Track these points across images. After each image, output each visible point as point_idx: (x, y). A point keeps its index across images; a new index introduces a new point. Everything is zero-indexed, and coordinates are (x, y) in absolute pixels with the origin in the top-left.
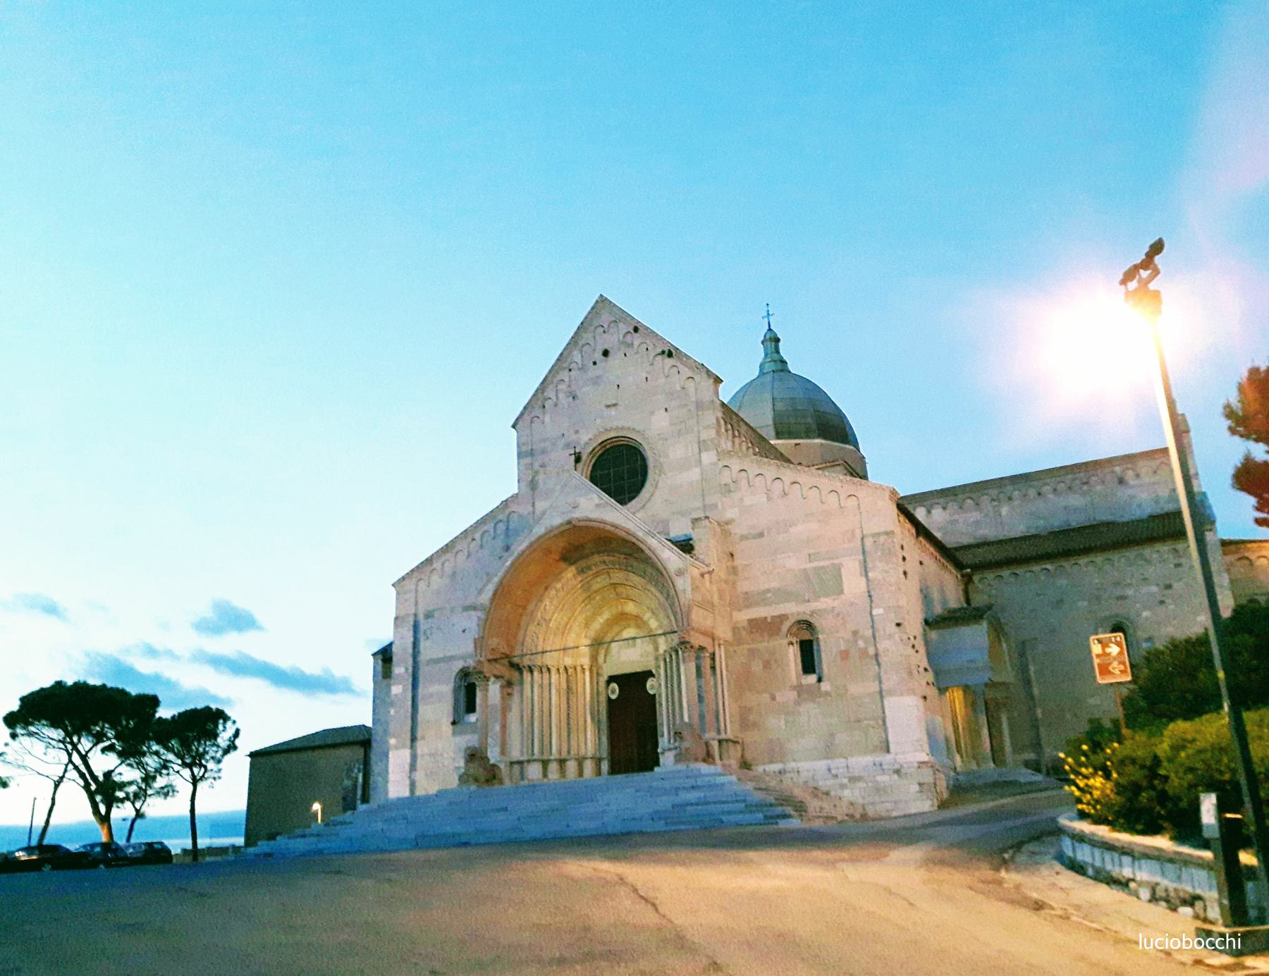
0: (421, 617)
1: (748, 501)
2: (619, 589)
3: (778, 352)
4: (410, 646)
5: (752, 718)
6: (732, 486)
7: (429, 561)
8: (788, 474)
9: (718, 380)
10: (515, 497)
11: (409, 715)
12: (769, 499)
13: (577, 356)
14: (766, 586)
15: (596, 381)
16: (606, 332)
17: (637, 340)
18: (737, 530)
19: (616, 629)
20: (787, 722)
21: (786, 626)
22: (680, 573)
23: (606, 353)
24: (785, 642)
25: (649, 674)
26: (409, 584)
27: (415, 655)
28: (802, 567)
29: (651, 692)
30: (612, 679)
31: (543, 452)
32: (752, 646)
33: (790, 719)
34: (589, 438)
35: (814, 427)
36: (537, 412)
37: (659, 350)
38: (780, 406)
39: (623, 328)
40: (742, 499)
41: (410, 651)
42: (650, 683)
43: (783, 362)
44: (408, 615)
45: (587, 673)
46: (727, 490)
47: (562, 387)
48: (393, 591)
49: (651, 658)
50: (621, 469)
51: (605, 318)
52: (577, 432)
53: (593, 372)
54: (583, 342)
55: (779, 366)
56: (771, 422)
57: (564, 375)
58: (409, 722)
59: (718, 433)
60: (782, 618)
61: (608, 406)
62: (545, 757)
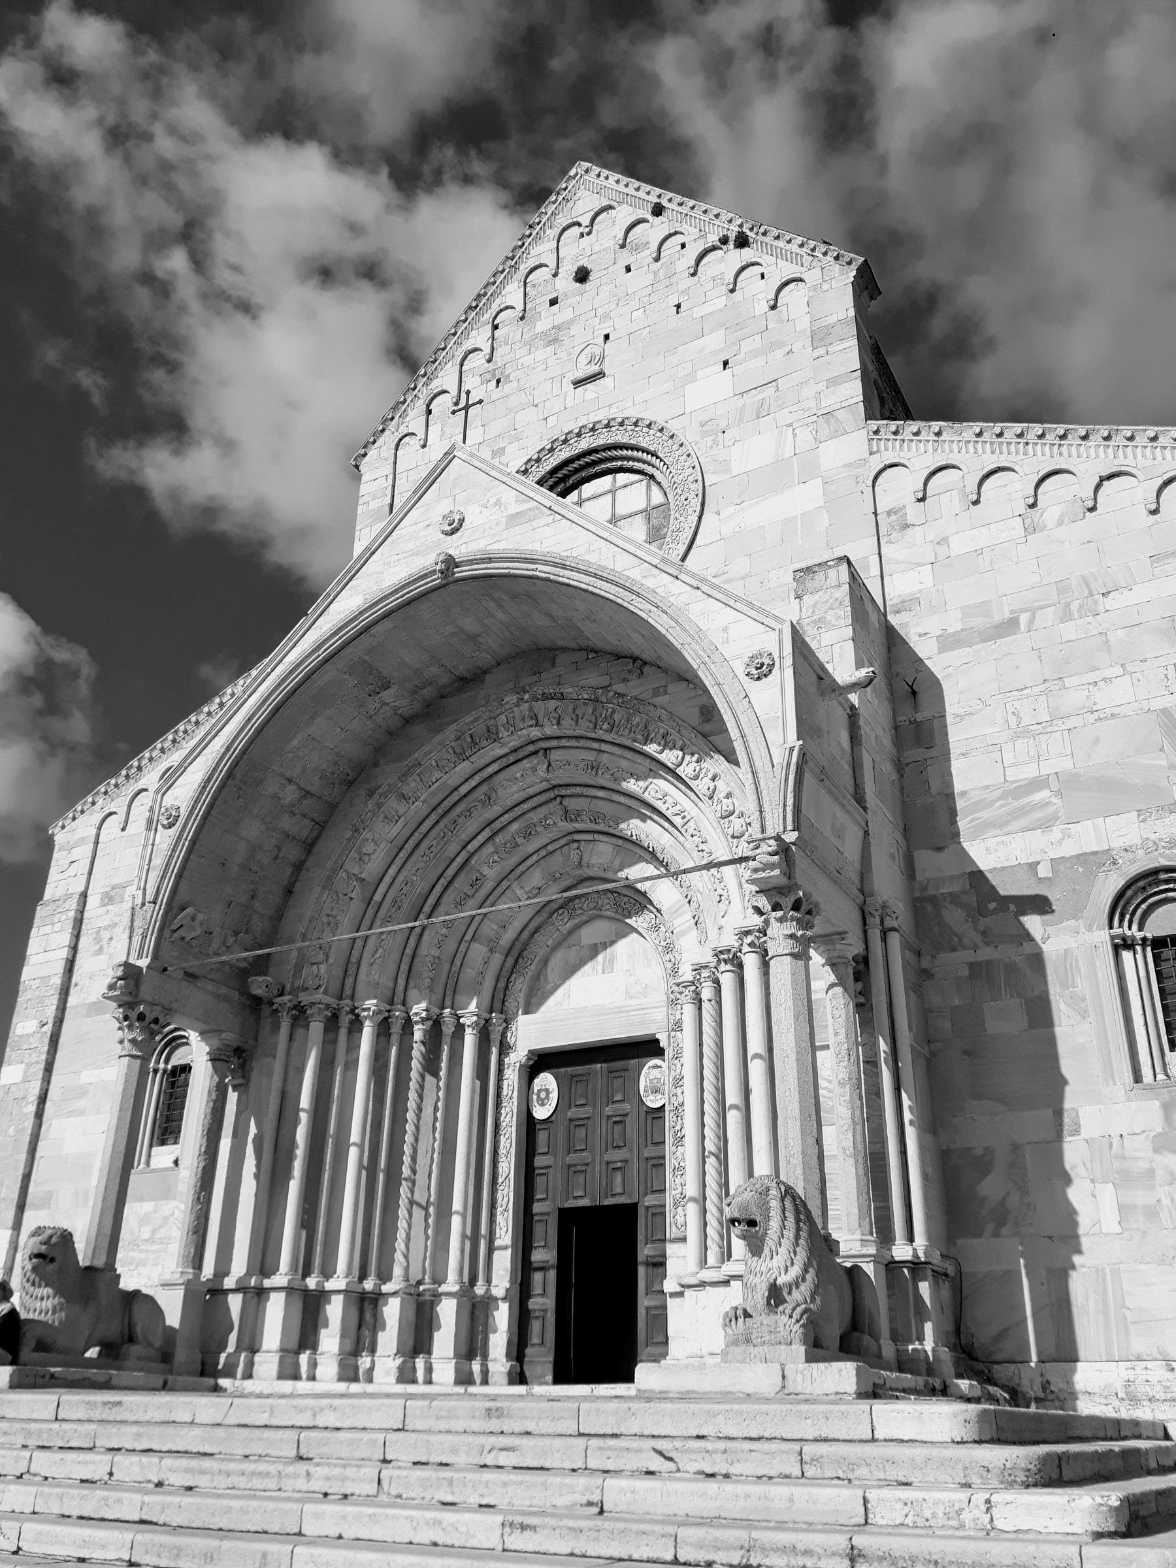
0: (93, 901)
1: (958, 545)
2: (572, 804)
4: (60, 967)
5: (991, 1188)
6: (913, 512)
8: (1088, 457)
11: (27, 1139)
12: (1030, 530)
14: (1030, 772)
15: (553, 338)
19: (563, 924)
20: (1124, 1210)
21: (1113, 883)
23: (582, 276)
24: (1102, 937)
25: (649, 1048)
27: (65, 992)
28: (1158, 704)
29: (653, 1102)
30: (541, 1061)
32: (986, 954)
33: (1139, 1197)
37: (713, 239)
40: (943, 541)
41: (57, 981)
42: (650, 1073)
44: (69, 896)
45: (470, 1041)
47: (476, 362)
49: (659, 998)
52: (502, 451)
53: (546, 319)
54: (531, 263)
58: (23, 1157)
60: (1094, 862)
61: (578, 383)
62: (312, 1282)
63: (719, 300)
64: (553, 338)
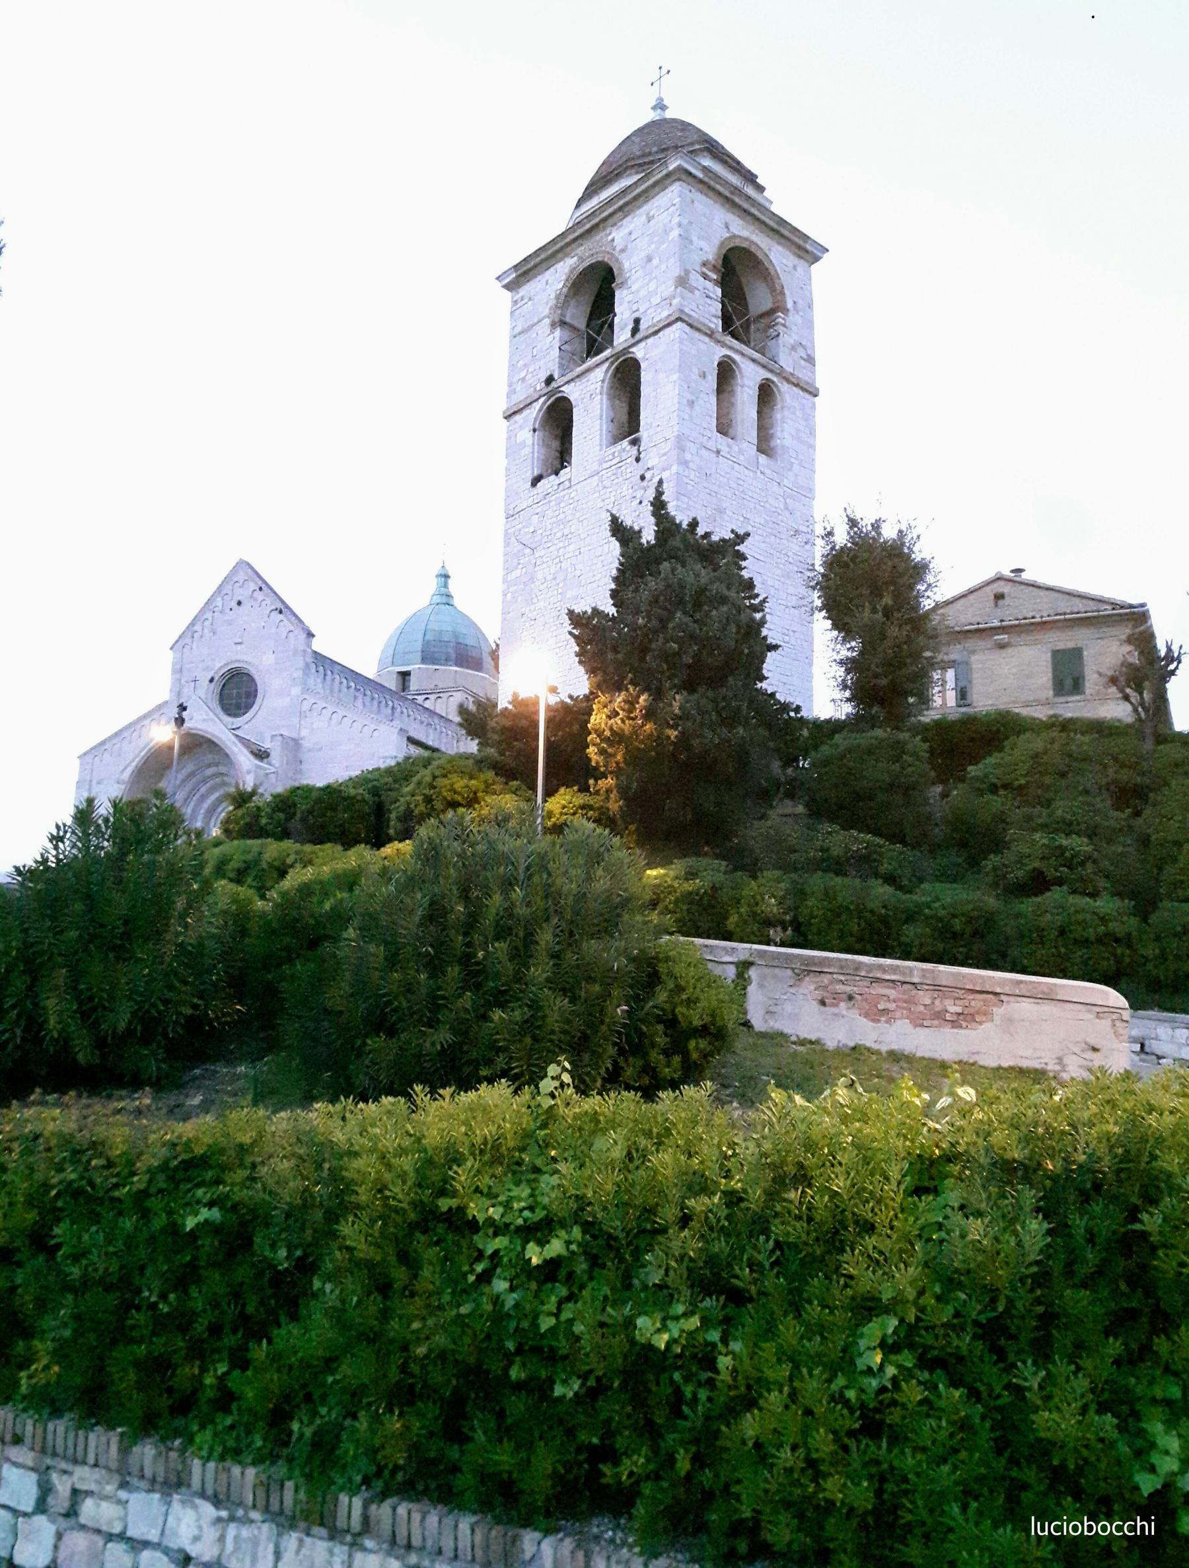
3: (446, 586)
7: (103, 743)
9: (310, 635)
10: (166, 702)
13: (219, 602)
15: (230, 623)
16: (246, 585)
17: (259, 596)
18: (306, 744)
22: (249, 772)
23: (239, 603)
26: (89, 758)
31: (190, 671)
34: (219, 665)
35: (453, 656)
36: (188, 640)
38: (428, 637)
39: (252, 586)
43: (449, 596)
46: (302, 715)
48: (78, 761)
50: (237, 691)
51: (241, 577)
53: (230, 616)
55: (444, 600)
56: (419, 646)
57: (209, 615)
59: (305, 674)
63: (273, 630)
64: (230, 623)
